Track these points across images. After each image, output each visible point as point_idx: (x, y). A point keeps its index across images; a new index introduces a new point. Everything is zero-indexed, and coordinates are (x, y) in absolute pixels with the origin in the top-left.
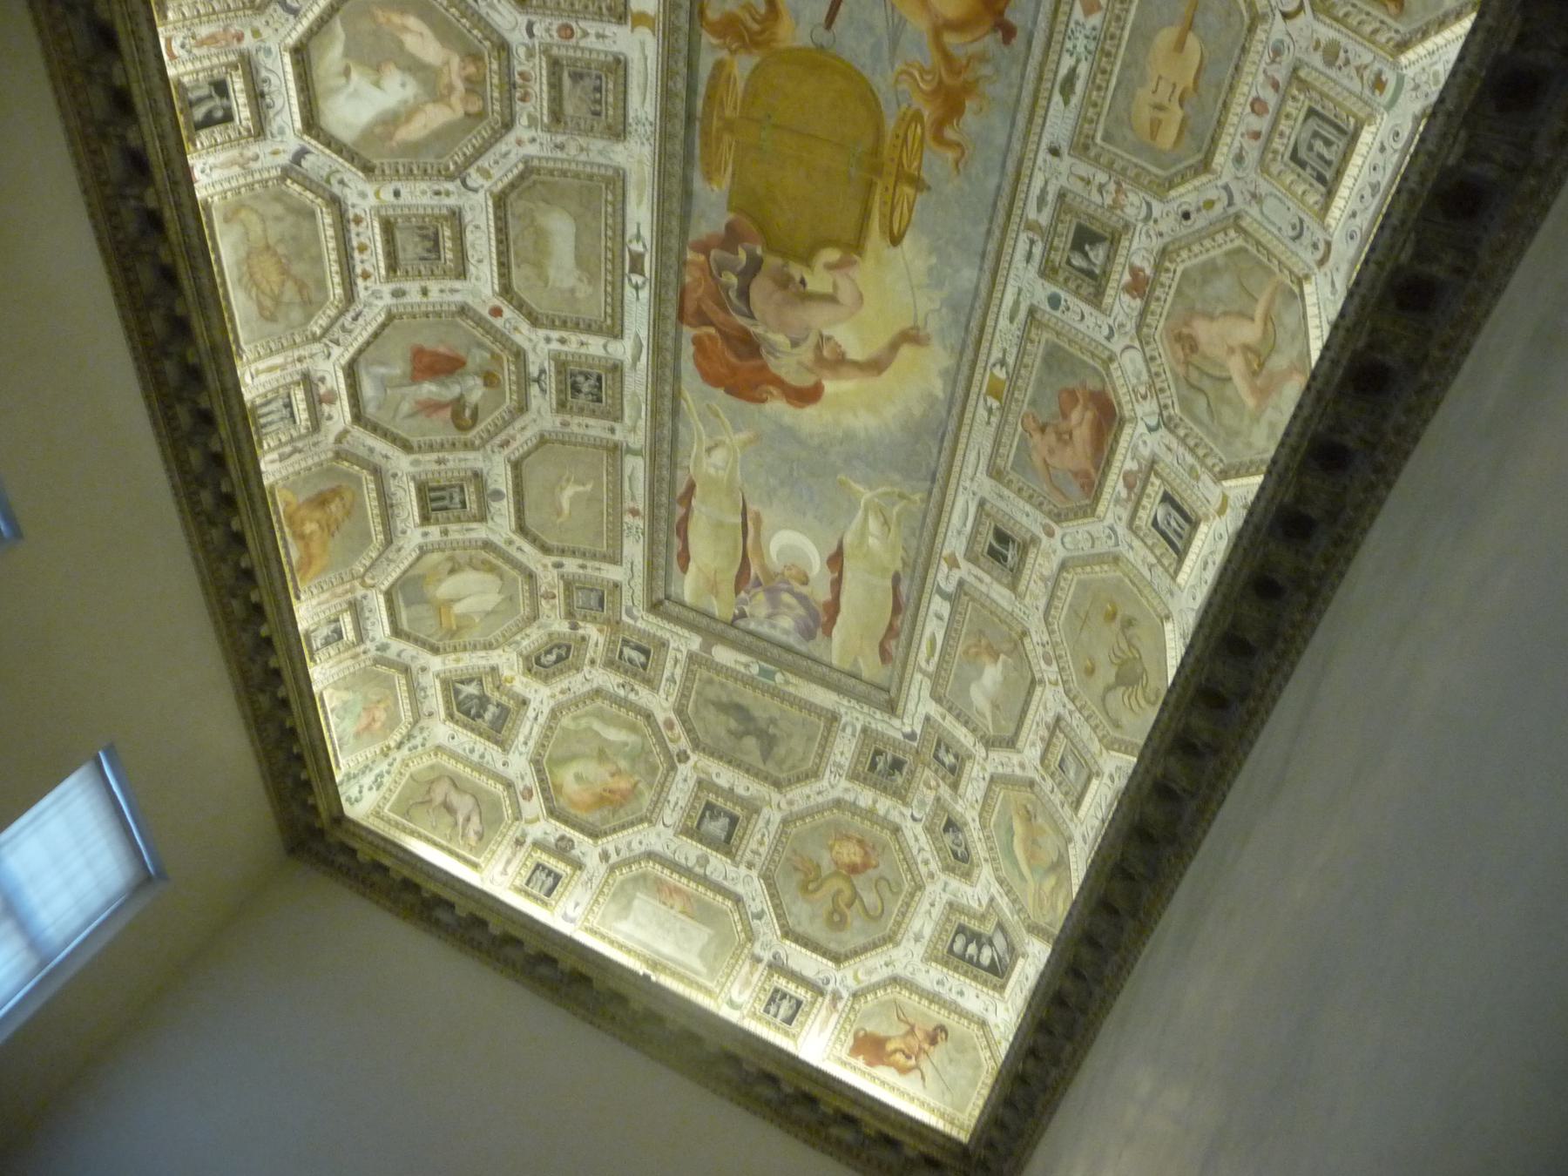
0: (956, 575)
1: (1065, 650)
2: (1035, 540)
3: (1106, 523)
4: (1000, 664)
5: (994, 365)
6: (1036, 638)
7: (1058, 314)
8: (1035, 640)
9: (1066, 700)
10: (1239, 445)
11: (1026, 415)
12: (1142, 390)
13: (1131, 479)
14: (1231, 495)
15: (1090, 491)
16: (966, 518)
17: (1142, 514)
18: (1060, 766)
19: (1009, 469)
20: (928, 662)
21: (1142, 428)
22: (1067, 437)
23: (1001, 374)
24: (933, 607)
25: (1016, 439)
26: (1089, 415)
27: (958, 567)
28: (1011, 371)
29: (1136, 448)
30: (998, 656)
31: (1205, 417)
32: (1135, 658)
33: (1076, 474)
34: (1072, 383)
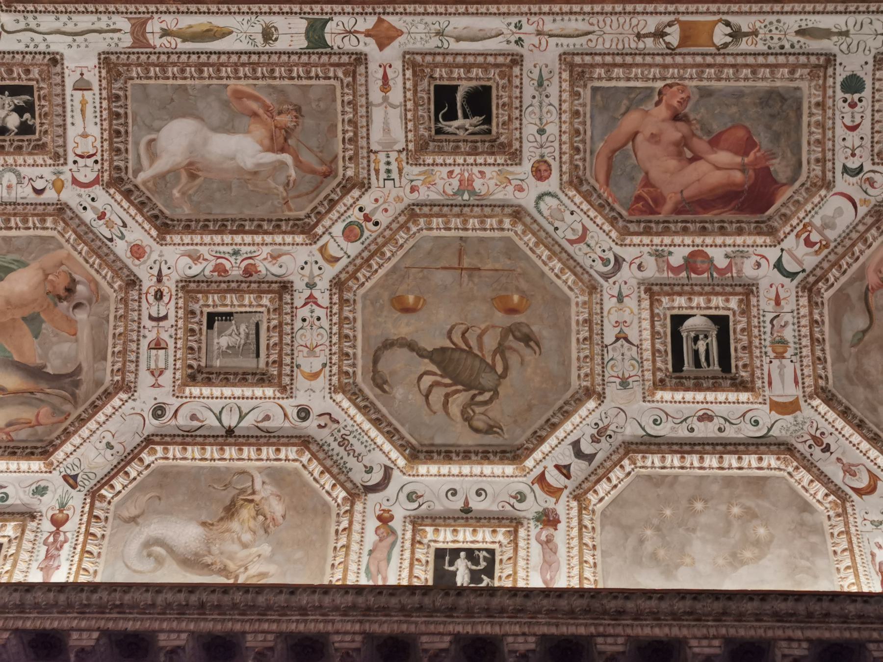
0: (369, 46)
1: (393, 257)
2: (515, 157)
3: (618, 250)
4: (271, 157)
5: (728, 24)
6: (367, 202)
7: (840, 94)
8: (361, 203)
9: (323, 284)
10: (861, 393)
11: (684, 89)
12: (815, 237)
13: (700, 264)
14: (806, 412)
15: (642, 212)
16: (473, 39)
17: (681, 301)
18: (212, 318)
19: (590, 85)
20: (165, 33)
21: (773, 254)
22: (689, 155)
23: (720, 35)
24: (279, 21)
25: (639, 84)
26: (738, 176)
27: (381, 46)
28: (731, 49)
29: (744, 255)
30: (282, 150)
31: (848, 335)
32: (493, 368)
33: (647, 182)
34: (763, 139)
